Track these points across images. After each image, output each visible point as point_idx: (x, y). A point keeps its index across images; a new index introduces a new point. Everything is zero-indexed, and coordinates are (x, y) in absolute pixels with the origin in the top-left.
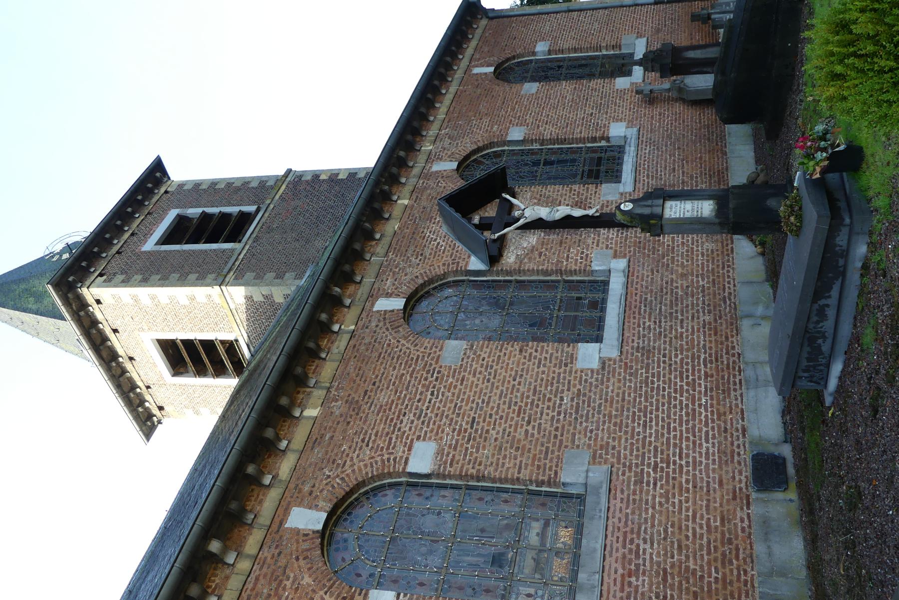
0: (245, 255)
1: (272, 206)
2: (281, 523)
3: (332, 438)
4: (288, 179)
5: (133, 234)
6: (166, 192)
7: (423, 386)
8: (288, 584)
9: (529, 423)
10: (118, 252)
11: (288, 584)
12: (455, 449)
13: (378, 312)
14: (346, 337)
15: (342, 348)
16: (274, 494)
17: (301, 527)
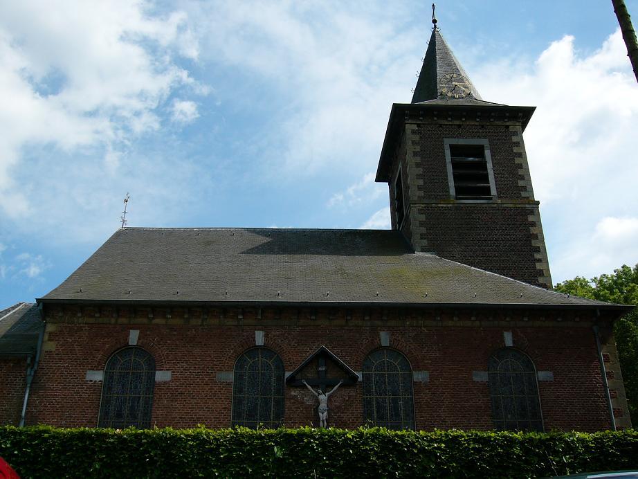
0: (442, 207)
1: (495, 205)
2: (131, 328)
3: (174, 335)
4: (527, 206)
5: (459, 126)
6: (507, 127)
7: (203, 368)
8: (106, 340)
9: (180, 418)
10: (441, 126)
11: (106, 340)
12: (167, 389)
13: (255, 334)
14: (236, 323)
15: (228, 324)
16: (145, 321)
17: (130, 336)
